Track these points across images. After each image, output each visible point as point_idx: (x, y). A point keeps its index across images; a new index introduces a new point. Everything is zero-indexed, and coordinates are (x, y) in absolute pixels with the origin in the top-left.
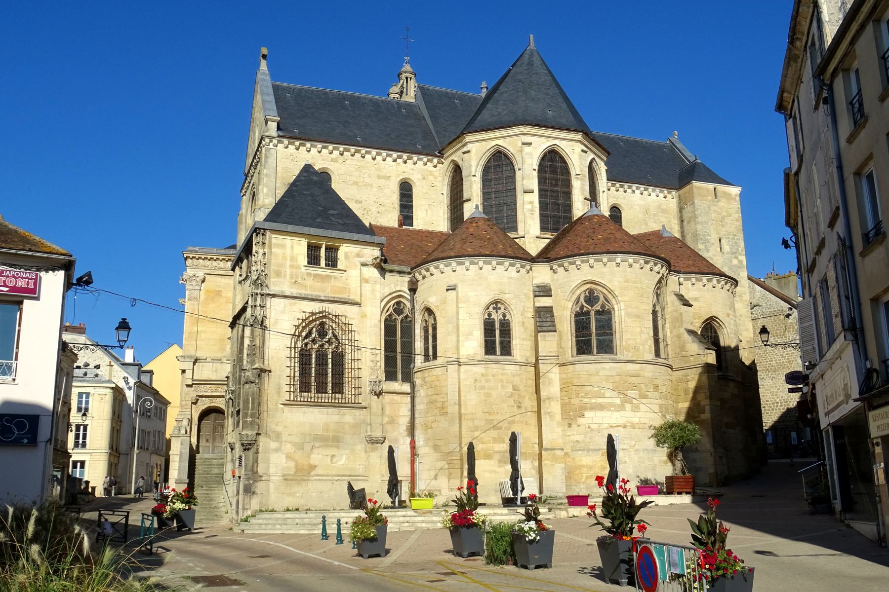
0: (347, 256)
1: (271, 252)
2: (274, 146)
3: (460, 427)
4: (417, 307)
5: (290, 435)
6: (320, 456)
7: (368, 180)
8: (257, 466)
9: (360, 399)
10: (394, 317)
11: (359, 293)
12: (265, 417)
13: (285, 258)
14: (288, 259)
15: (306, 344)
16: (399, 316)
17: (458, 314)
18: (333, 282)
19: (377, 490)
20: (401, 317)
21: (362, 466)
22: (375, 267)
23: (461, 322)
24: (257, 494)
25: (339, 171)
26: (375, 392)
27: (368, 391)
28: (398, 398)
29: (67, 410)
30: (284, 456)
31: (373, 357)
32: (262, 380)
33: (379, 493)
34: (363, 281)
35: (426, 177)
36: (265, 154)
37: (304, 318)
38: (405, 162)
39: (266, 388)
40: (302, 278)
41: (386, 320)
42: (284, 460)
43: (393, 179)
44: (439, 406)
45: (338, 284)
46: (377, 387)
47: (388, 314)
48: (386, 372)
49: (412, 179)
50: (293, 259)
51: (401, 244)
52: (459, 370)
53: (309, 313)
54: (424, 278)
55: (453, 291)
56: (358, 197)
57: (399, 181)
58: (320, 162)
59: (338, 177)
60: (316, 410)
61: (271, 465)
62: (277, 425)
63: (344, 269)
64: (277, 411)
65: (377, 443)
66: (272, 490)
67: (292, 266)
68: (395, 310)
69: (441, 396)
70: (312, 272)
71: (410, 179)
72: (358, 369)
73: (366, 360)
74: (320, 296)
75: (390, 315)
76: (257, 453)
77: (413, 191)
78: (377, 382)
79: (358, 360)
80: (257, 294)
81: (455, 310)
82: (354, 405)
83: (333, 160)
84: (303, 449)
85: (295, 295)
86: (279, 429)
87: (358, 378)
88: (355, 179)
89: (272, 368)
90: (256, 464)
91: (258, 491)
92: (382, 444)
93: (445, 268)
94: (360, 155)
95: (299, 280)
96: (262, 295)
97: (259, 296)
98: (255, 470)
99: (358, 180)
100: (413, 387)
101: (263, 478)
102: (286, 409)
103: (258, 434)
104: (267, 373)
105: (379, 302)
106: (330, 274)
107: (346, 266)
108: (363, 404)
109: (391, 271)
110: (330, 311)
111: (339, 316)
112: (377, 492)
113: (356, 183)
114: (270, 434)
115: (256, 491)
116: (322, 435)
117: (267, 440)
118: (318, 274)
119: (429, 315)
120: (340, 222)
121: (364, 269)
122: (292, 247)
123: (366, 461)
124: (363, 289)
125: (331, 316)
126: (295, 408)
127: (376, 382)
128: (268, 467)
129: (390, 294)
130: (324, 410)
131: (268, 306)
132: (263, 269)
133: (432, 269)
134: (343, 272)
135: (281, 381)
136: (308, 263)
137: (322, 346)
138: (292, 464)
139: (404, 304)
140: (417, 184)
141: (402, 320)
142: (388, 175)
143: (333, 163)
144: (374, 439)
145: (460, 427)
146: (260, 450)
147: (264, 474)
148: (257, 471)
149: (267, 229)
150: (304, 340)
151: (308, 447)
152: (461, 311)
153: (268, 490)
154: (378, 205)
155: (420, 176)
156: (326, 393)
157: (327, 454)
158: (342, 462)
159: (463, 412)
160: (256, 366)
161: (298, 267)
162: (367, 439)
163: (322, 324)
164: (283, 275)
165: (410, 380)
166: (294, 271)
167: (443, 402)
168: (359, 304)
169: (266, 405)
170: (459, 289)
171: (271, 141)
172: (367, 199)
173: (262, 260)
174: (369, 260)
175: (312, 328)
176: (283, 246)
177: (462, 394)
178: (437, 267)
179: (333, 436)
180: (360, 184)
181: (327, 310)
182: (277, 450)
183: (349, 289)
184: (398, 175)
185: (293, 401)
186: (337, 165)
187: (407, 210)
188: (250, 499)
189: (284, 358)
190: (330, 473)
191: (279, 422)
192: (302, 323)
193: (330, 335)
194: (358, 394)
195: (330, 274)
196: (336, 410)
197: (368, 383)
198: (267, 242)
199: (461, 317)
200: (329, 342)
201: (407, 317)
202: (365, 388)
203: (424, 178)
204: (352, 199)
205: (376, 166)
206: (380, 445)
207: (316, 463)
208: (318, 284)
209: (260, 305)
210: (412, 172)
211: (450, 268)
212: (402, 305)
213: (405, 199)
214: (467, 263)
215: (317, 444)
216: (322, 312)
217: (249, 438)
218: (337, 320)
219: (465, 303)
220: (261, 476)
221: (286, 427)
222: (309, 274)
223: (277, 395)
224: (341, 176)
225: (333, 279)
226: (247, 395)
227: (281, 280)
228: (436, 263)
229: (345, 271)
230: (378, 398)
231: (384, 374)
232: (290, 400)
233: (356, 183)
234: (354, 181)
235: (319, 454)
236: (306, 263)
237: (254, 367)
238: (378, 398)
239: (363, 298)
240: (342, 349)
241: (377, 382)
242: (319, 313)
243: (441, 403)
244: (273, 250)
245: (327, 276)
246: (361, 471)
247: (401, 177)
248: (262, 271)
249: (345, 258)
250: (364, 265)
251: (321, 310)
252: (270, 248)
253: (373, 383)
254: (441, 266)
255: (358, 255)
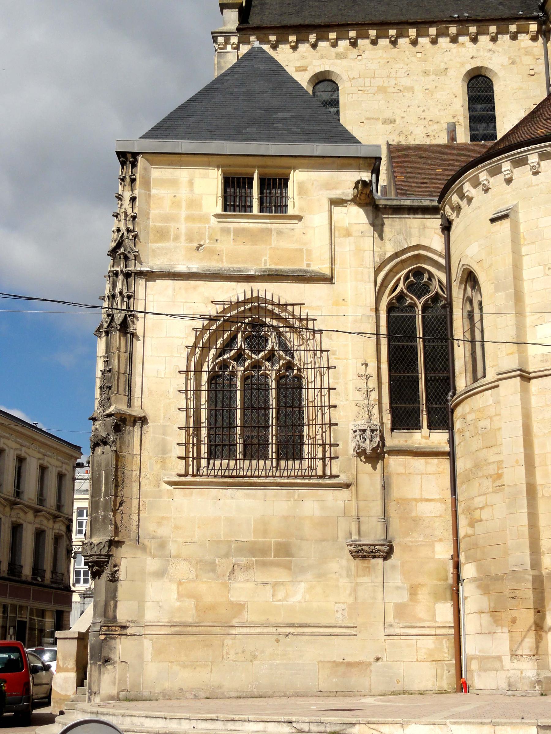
0: (302, 190)
1: (149, 195)
2: (234, 48)
3: (533, 517)
4: (453, 277)
5: (186, 543)
6: (250, 585)
7: (406, 82)
8: (115, 607)
9: (335, 468)
10: (408, 301)
11: (327, 256)
12: (134, 510)
13: (176, 204)
14: (184, 204)
15: (224, 365)
16: (419, 298)
17: (517, 268)
18: (274, 241)
19: (374, 656)
20: (423, 300)
21: (341, 605)
22: (360, 205)
23: (527, 287)
24: (114, 663)
25: (350, 73)
26: (364, 451)
27: (351, 451)
28: (419, 463)
29: (64, 528)
30: (174, 587)
31: (361, 383)
32: (127, 438)
33: (379, 663)
34: (337, 234)
35: (518, 60)
36: (219, 63)
37: (214, 313)
38: (474, 40)
39: (136, 451)
40: (210, 238)
41: (391, 309)
42: (175, 595)
43: (452, 73)
44: (491, 472)
45: (284, 244)
46: (368, 441)
47: (394, 294)
48: (393, 411)
49: (490, 66)
50: (193, 203)
51: (439, 167)
52: (525, 392)
53: (224, 303)
54: (458, 209)
55: (505, 224)
56: (388, 114)
57: (465, 75)
58: (315, 62)
59: (348, 84)
60: (240, 493)
61: (148, 604)
62: (159, 524)
63: (297, 213)
64: (160, 497)
65: (374, 557)
66: (148, 655)
67: (190, 218)
68: (410, 287)
69: (494, 450)
70: (232, 226)
71: (486, 68)
72: (330, 407)
73: (346, 389)
74: (248, 270)
75: (401, 297)
76: (114, 579)
77: (495, 88)
78: (368, 432)
79: (330, 389)
80: (116, 274)
81: (509, 260)
82: (321, 481)
83: (339, 56)
84: (214, 570)
85: (194, 270)
86: (164, 531)
87: (331, 425)
88: (381, 84)
89: (149, 411)
90: (112, 603)
91: (116, 656)
92: (385, 558)
93: (492, 180)
94: (388, 40)
95: (206, 243)
96: (127, 275)
97: (121, 277)
98: (110, 614)
99: (386, 84)
100: (451, 441)
101: (128, 631)
102: (178, 492)
103: (114, 543)
104: (139, 423)
105: (372, 271)
106: (269, 226)
107: (301, 209)
108: (343, 479)
109: (398, 210)
110: (269, 297)
111: (286, 305)
112: (378, 659)
113: (382, 90)
114: (146, 543)
115: (112, 656)
116: (254, 543)
117: (139, 554)
118: (244, 229)
119: (473, 288)
120: (294, 129)
121: (337, 210)
122: (191, 183)
123: (350, 595)
124: (337, 248)
125: (270, 307)
126: (196, 492)
127: (364, 431)
128: (141, 609)
129: (396, 255)
130: (259, 492)
131: (140, 293)
132: (131, 227)
133: (467, 187)
134: (296, 221)
135: (168, 438)
136: (225, 210)
137: (256, 366)
138: (190, 603)
139: (430, 274)
140: (501, 73)
141: (425, 308)
142: (443, 66)
143: (339, 61)
144: (366, 548)
145: (533, 517)
146: (122, 575)
147: (131, 622)
148: (115, 617)
149: (138, 154)
150: (221, 355)
151: (224, 566)
152: (526, 261)
153: (140, 656)
154: (426, 122)
155: (506, 61)
156: (266, 458)
157: (265, 580)
158: (298, 597)
159: (539, 480)
160: (112, 409)
161: (203, 219)
162: (351, 548)
163: (257, 325)
164: (172, 237)
165: (448, 425)
166: (196, 226)
167: (498, 462)
168: (328, 280)
169: (135, 485)
170: (522, 216)
171: (227, 42)
172: (404, 115)
173: (129, 211)
174: (349, 192)
175: (237, 331)
176: (174, 183)
177: (536, 442)
178: (476, 184)
179: (278, 544)
180: (390, 90)
181: (262, 295)
182: (161, 574)
183: (309, 252)
184: (463, 64)
185: (193, 476)
186: (345, 62)
187: (484, 125)
188: (100, 673)
189: (173, 391)
190: (272, 620)
191: (163, 518)
192: (210, 325)
193: (272, 343)
194: (331, 458)
195: (269, 226)
196: (283, 492)
197: (352, 435)
198: (138, 176)
199: (526, 274)
200: (270, 357)
201: (436, 298)
202: (346, 443)
203: (513, 63)
204: (378, 119)
205: (419, 55)
206: (380, 561)
207: (242, 599)
208: (244, 249)
209: (121, 293)
210: (489, 54)
211: (500, 178)
212: (426, 275)
213: (479, 106)
214: (533, 159)
215: (243, 561)
216: (251, 300)
217: (96, 551)
218: (283, 315)
219: (534, 243)
220: (124, 627)
221: (177, 527)
222: (226, 231)
223: (159, 466)
224: (353, 81)
225: (274, 235)
226: (100, 466)
227: (170, 244)
228: (471, 173)
229: (299, 218)
230: (375, 468)
231: (389, 416)
232: (185, 475)
233: (382, 90)
234: (378, 87)
235: (248, 580)
236: (219, 209)
237: (107, 412)
238: (375, 468)
239: (337, 268)
240: (299, 370)
241: (368, 432)
242: (245, 302)
243: (495, 466)
244: (154, 191)
245: (262, 230)
246: (339, 615)
247: (469, 67)
248: (128, 231)
249: (299, 194)
250: (336, 202)
251: (248, 296)
252: (147, 184)
253: (359, 433)
254: (483, 176)
255: (327, 186)
